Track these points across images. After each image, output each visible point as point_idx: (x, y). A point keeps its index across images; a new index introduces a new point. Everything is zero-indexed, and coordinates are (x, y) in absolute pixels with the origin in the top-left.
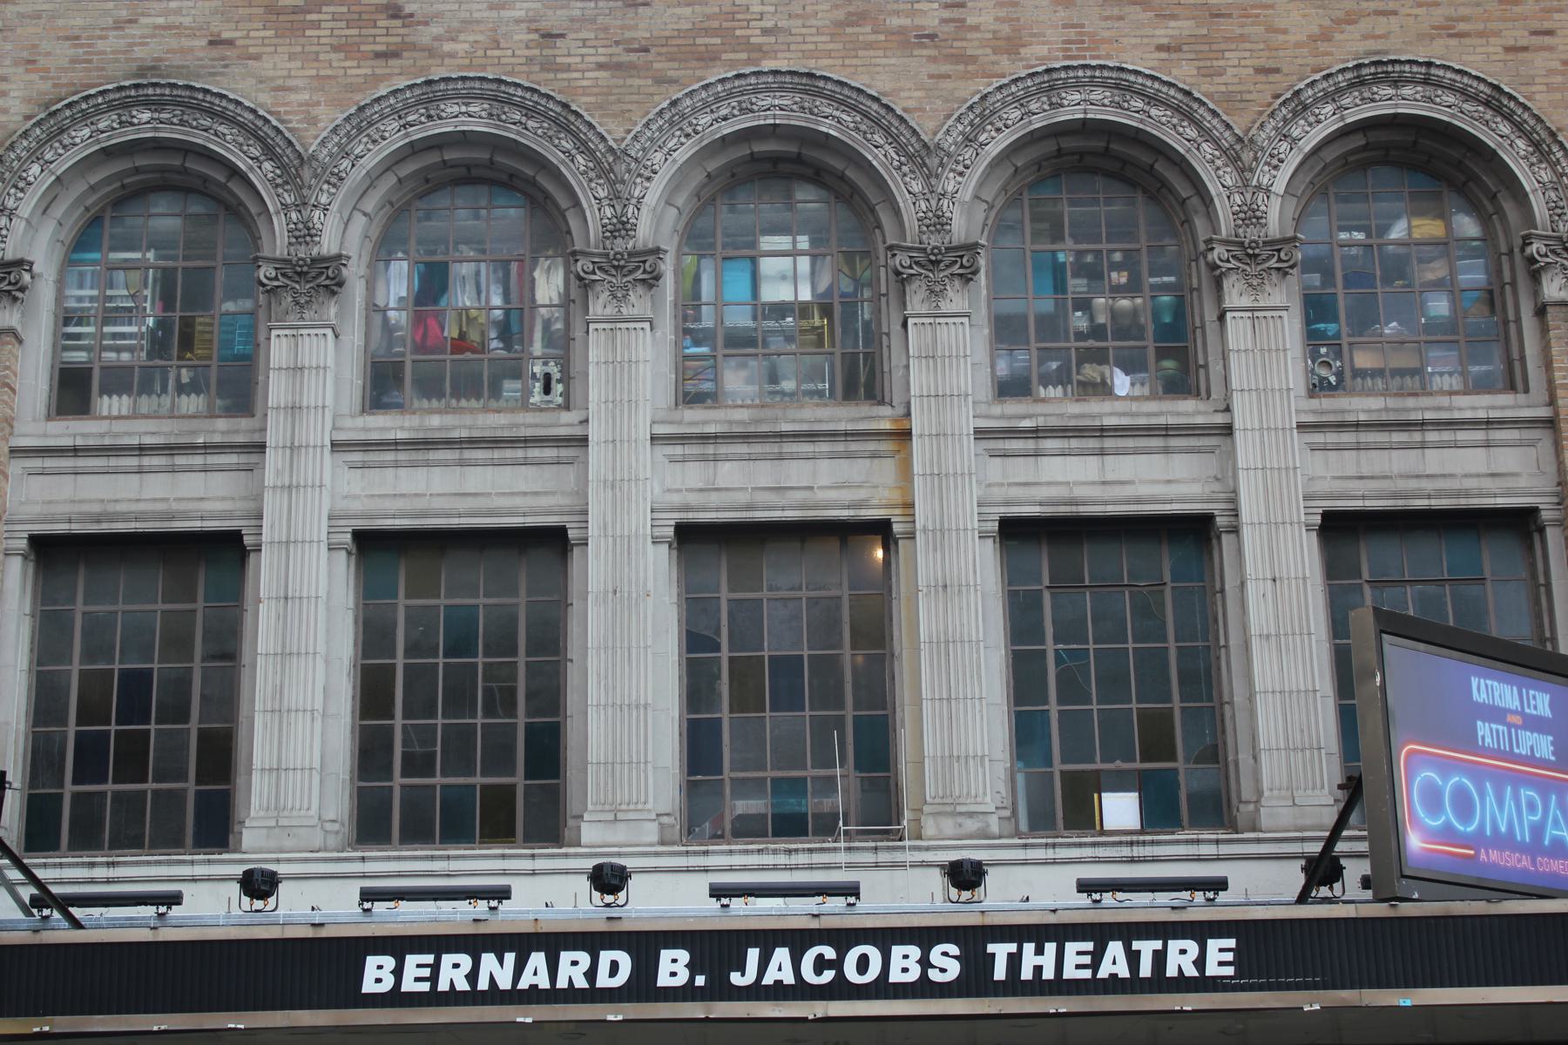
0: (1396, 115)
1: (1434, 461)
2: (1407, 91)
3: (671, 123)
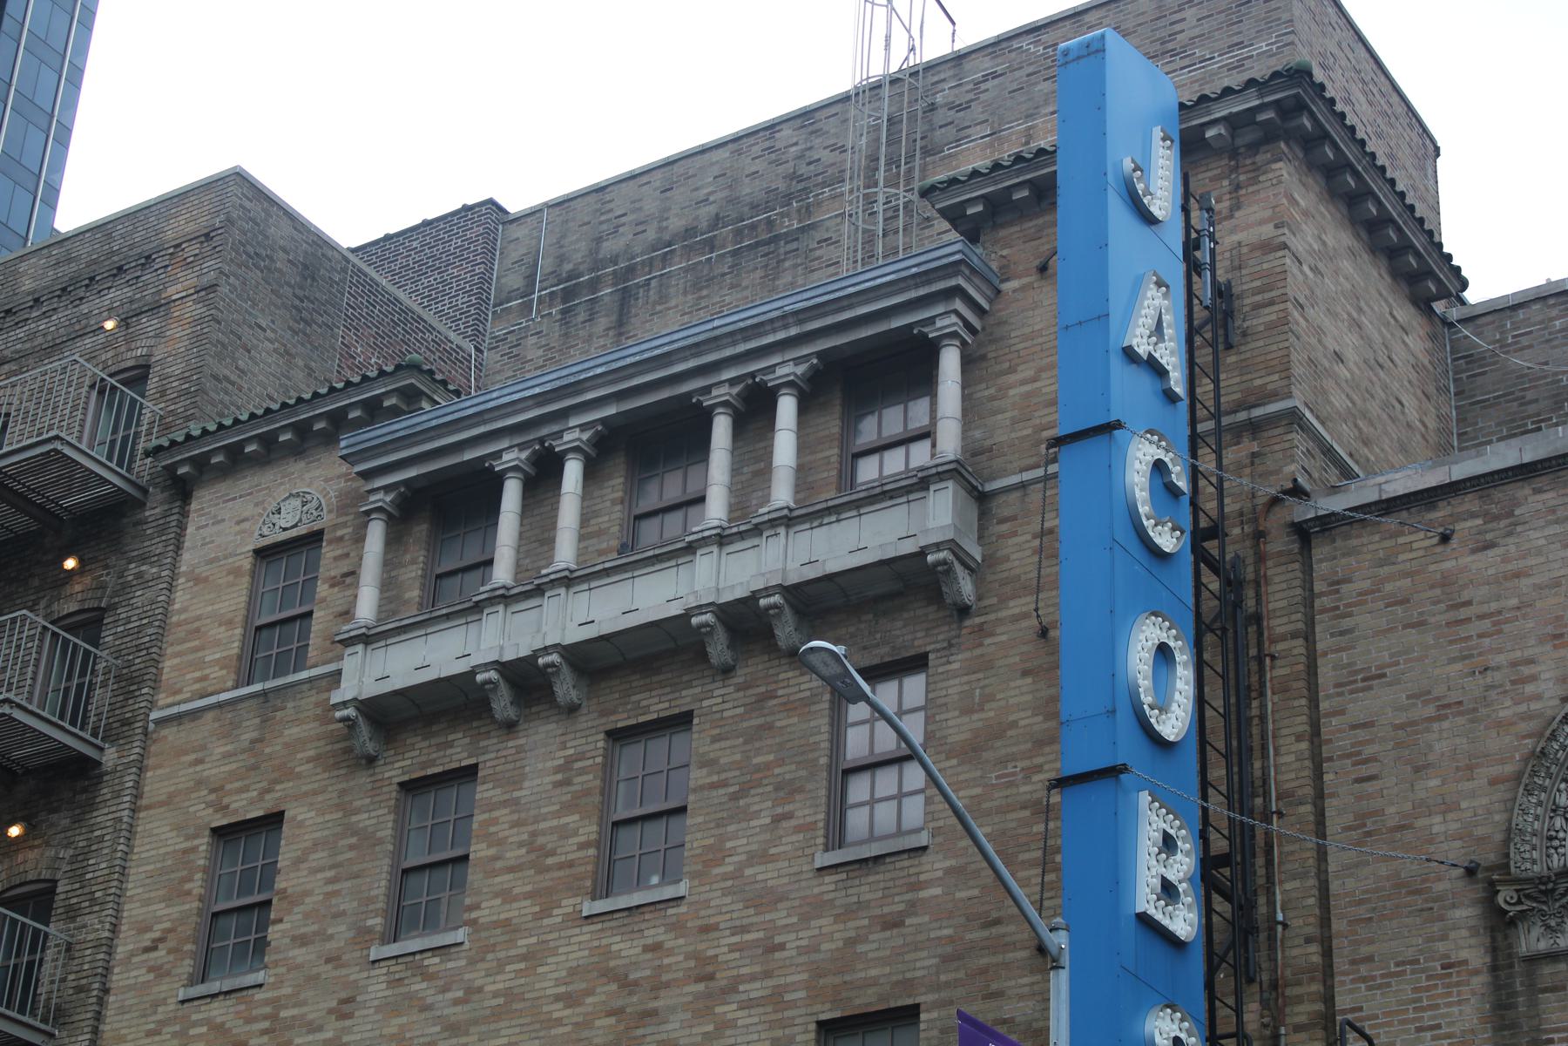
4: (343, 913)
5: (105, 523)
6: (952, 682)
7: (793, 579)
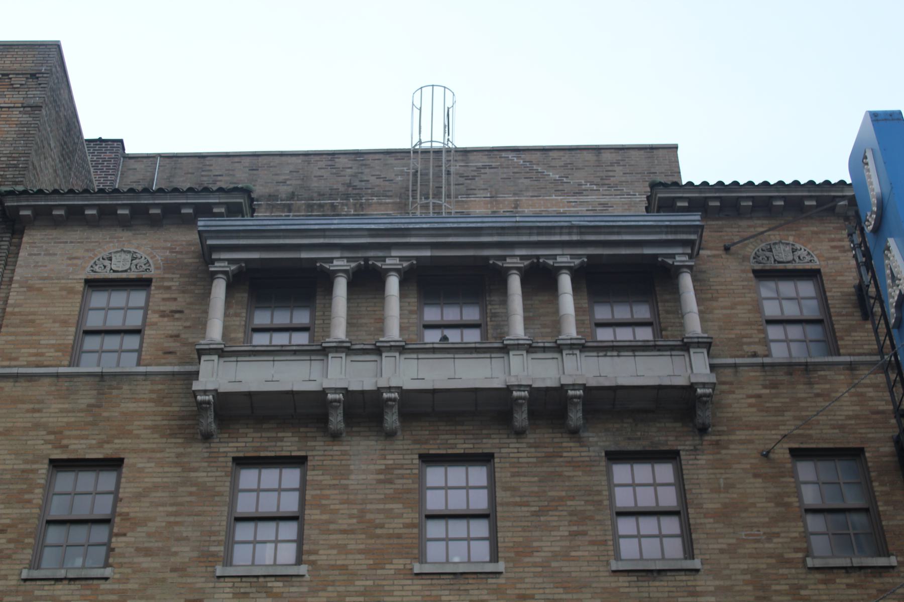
4: (187, 539)
6: (701, 471)
7: (592, 383)
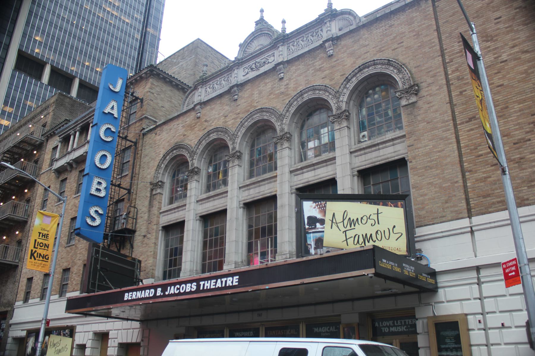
0: (370, 74)
1: (382, 152)
2: (371, 68)
3: (242, 126)
5: (40, 146)
